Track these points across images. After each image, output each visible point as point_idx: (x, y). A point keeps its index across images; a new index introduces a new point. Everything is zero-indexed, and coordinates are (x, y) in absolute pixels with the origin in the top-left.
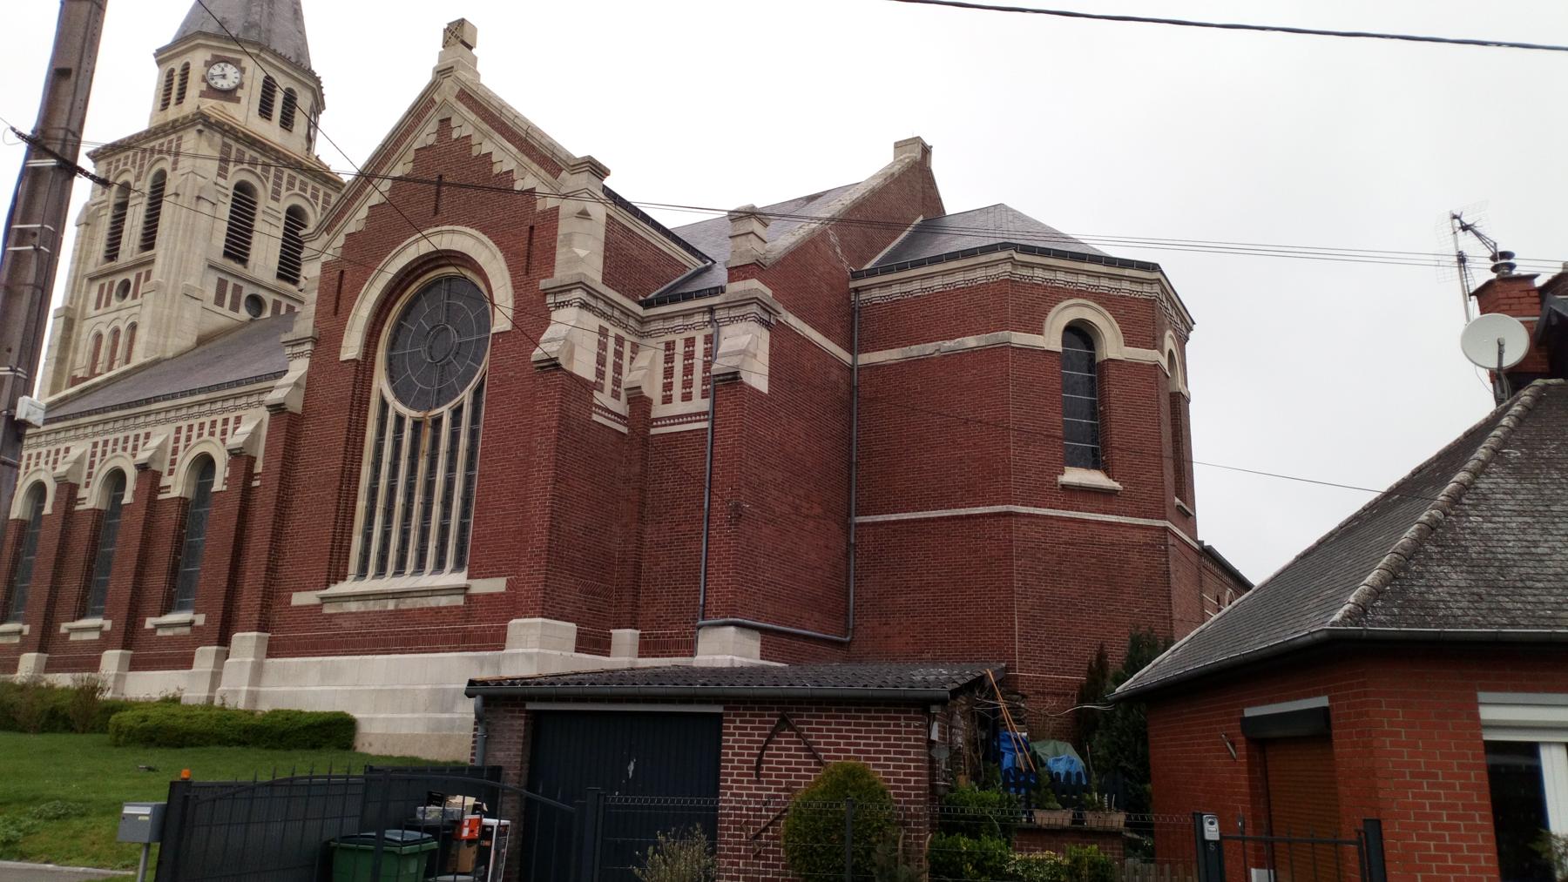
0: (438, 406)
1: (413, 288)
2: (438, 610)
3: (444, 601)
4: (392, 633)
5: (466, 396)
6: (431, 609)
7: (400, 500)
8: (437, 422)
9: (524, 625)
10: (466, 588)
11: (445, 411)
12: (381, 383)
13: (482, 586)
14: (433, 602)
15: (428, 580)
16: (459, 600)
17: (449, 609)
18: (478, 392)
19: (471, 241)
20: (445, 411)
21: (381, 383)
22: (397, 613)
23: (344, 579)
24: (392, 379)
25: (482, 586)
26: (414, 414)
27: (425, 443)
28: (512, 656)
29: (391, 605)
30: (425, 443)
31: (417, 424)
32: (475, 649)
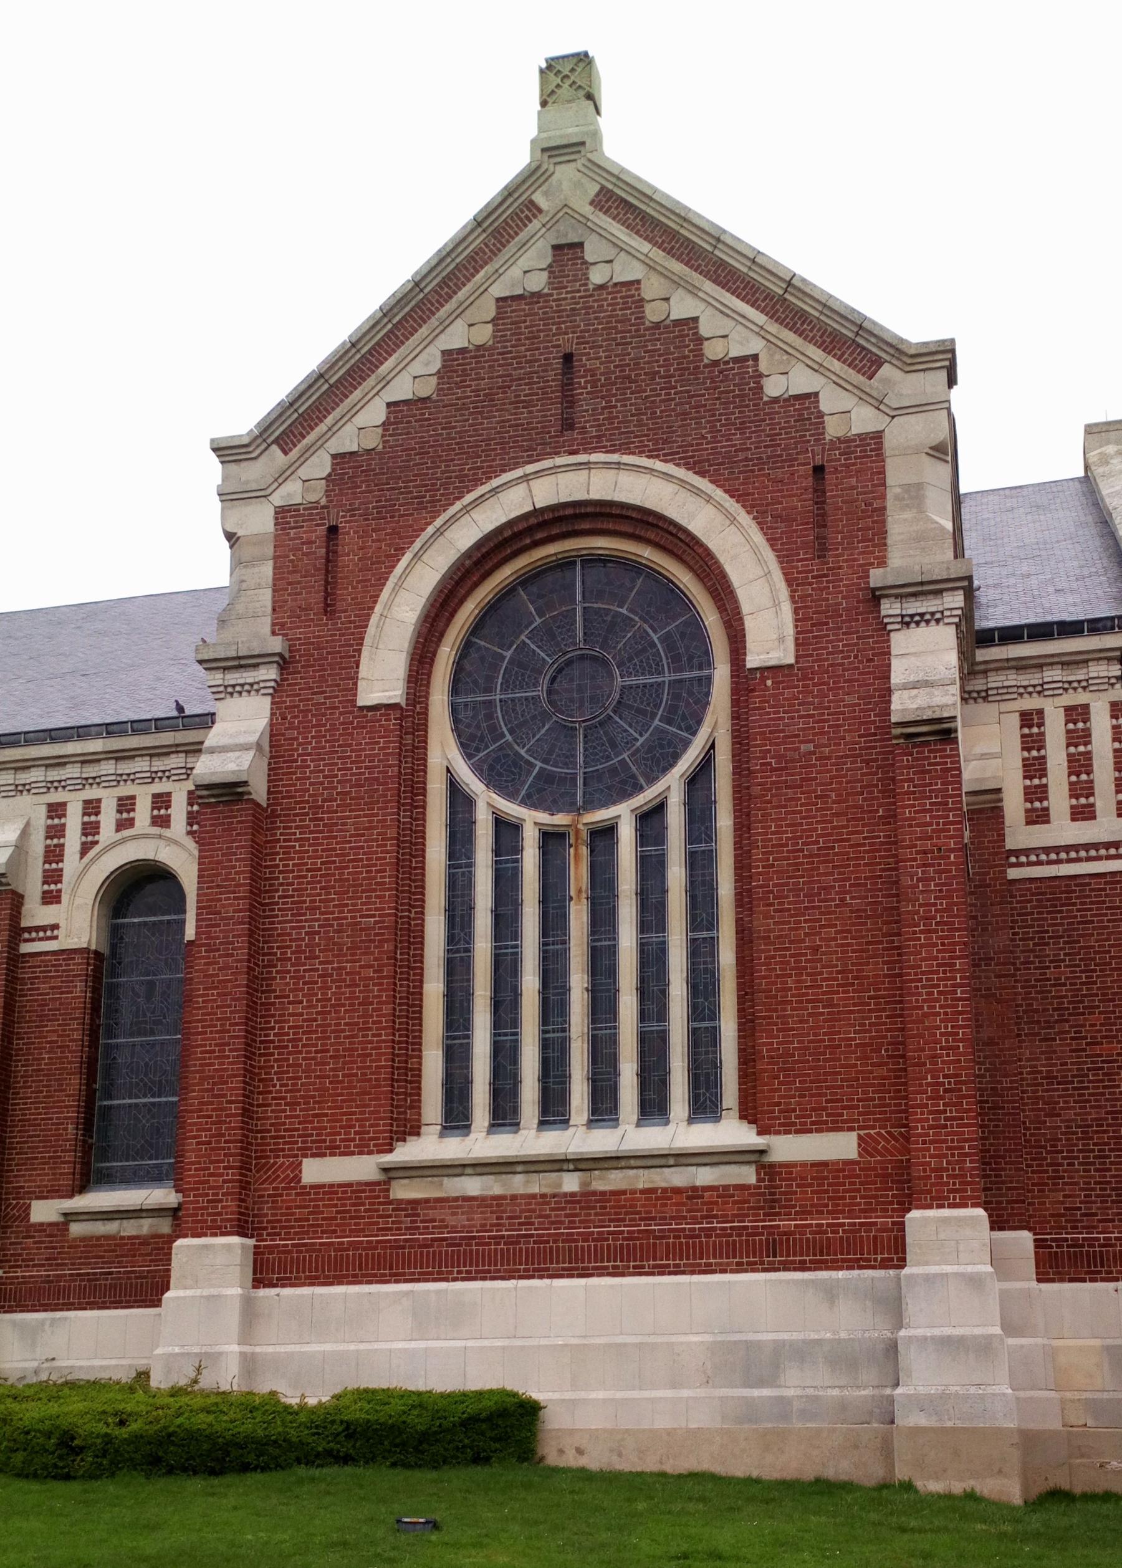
0: (590, 804)
1: (506, 573)
2: (695, 1192)
3: (705, 1176)
4: (586, 1237)
5: (672, 785)
6: (677, 1191)
7: (530, 982)
8: (606, 834)
9: (945, 1220)
10: (762, 1152)
11: (623, 815)
12: (444, 752)
13: (790, 1148)
14: (678, 1178)
15: (630, 1135)
16: (748, 1175)
17: (723, 1192)
18: (699, 779)
19: (670, 488)
20: (623, 815)
21: (444, 752)
22: (586, 1199)
23: (414, 1130)
24: (468, 745)
25: (790, 1148)
26: (543, 817)
27: (579, 875)
28: (929, 1279)
29: (571, 1183)
30: (579, 875)
31: (550, 839)
32: (802, 1267)
